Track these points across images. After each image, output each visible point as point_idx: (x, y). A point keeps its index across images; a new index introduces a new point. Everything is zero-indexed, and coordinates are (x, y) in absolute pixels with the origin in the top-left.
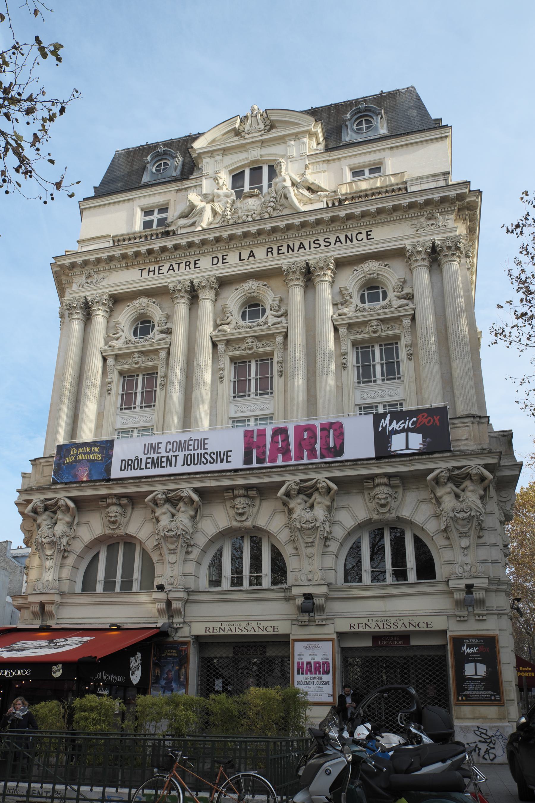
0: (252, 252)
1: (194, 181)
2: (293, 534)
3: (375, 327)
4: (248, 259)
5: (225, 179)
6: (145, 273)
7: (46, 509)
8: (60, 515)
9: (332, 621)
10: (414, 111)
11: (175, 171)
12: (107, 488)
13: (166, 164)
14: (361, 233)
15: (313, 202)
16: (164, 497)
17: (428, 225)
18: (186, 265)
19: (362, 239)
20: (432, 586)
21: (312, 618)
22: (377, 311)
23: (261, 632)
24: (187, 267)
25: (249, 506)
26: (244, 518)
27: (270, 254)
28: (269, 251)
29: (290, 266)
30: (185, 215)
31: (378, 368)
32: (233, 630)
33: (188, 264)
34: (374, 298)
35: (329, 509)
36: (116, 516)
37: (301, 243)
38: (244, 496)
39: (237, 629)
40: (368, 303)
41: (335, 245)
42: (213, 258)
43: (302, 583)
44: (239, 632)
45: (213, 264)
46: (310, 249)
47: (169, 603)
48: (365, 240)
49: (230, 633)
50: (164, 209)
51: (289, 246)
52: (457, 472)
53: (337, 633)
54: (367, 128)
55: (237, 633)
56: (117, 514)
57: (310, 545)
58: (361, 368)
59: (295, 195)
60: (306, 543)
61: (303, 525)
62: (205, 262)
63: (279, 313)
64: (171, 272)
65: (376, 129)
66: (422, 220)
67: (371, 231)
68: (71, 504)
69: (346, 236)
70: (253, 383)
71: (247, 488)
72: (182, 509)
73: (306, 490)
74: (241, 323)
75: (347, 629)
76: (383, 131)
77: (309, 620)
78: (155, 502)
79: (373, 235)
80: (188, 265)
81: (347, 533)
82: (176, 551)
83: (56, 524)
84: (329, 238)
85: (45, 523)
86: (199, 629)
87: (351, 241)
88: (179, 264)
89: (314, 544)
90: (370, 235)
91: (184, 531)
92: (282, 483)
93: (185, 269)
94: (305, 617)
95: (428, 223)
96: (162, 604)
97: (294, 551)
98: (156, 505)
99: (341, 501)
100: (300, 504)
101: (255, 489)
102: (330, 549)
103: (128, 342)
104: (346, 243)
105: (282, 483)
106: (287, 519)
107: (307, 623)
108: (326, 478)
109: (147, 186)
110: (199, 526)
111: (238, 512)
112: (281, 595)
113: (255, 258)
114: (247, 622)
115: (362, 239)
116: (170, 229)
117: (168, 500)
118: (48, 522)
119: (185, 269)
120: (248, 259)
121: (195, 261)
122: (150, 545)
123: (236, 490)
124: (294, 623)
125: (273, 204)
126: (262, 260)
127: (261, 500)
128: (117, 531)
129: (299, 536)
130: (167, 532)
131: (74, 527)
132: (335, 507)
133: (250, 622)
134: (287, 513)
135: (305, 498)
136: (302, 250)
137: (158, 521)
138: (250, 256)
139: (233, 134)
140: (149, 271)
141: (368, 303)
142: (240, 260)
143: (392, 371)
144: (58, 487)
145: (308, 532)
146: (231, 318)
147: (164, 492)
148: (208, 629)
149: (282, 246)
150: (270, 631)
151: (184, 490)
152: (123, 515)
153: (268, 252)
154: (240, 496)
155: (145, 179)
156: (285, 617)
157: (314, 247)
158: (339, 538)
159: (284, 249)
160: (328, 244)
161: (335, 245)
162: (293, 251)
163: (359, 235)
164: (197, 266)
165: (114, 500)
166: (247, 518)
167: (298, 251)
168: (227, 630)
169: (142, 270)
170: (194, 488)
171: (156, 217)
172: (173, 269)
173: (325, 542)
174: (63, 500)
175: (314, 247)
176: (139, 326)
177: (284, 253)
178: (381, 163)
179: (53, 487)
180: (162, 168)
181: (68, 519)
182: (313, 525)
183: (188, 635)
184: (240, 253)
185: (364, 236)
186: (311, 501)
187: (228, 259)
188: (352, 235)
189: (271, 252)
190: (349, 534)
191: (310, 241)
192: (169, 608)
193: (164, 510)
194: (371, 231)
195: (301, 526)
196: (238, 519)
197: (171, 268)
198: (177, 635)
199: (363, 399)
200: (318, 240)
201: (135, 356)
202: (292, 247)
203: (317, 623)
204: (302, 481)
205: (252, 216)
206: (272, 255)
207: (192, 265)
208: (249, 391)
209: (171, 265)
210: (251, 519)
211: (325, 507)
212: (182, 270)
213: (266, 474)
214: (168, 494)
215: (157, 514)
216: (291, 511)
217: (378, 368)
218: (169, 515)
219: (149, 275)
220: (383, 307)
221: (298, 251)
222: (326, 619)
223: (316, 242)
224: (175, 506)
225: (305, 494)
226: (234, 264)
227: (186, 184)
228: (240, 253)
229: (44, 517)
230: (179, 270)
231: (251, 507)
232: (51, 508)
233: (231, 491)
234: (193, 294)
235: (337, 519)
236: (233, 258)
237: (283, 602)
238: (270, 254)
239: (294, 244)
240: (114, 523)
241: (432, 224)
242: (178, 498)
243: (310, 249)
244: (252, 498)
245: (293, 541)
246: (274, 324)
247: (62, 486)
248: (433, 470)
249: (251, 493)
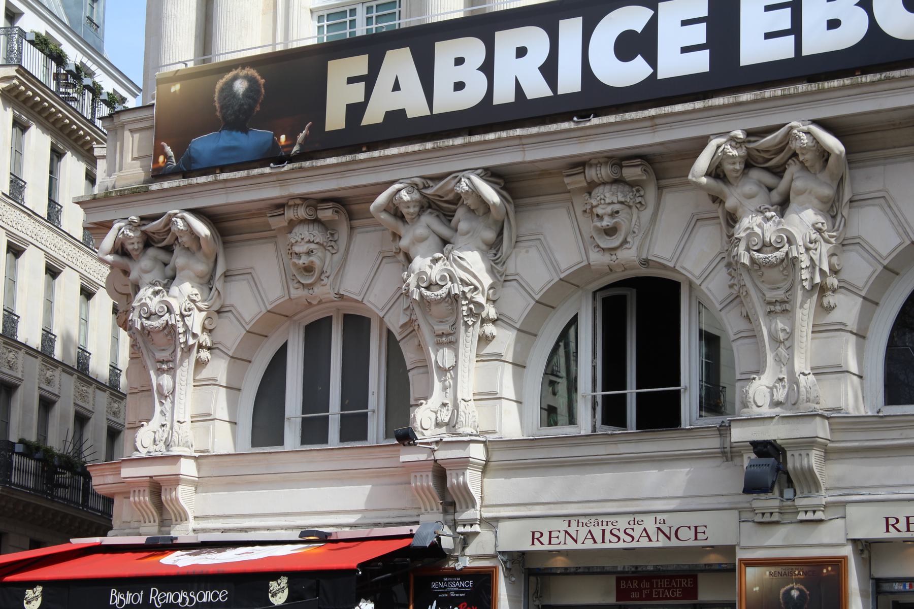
2: (736, 282)
7: (148, 242)
8: (179, 259)
9: (839, 512)
12: (282, 180)
16: (416, 196)
21: (789, 503)
23: (662, 542)
25: (630, 207)
26: (615, 242)
32: (599, 538)
35: (831, 209)
36: (309, 253)
38: (615, 182)
39: (608, 536)
43: (754, 411)
44: (611, 544)
49: (589, 545)
53: (855, 541)
55: (607, 545)
56: (312, 246)
57: (778, 308)
60: (770, 303)
61: (756, 254)
68: (202, 229)
71: (618, 160)
72: (463, 226)
73: (766, 156)
75: (878, 532)
77: (780, 508)
78: (395, 211)
81: (880, 268)
83: (173, 278)
85: (148, 278)
86: (512, 537)
89: (788, 307)
91: (467, 284)
92: (702, 142)
94: (769, 503)
96: (424, 474)
97: (743, 325)
98: (398, 215)
99: (868, 181)
100: (751, 197)
101: (638, 162)
102: (835, 317)
106: (725, 238)
107: (776, 518)
108: (816, 122)
110: (510, 268)
111: (599, 224)
112: (713, 443)
114: (631, 518)
117: (428, 205)
118: (155, 275)
122: (395, 321)
123: (591, 166)
124: (746, 516)
127: (660, 188)
128: (318, 291)
129: (749, 285)
131: (218, 284)
132: (847, 198)
133: (638, 517)
134: (722, 220)
135: (768, 179)
137: (409, 260)
144: (166, 185)
145: (775, 274)
147: (414, 186)
148: (537, 535)
150: (687, 539)
151: (460, 174)
152: (330, 245)
154: (604, 183)
156: (723, 502)
158: (860, 285)
165: (302, 213)
166: (625, 242)
168: (583, 540)
170: (486, 169)
174: (183, 218)
179: (155, 187)
181: (201, 267)
182: (780, 254)
183: (490, 551)
186: (783, 185)
193: (420, 229)
195: (752, 260)
196: (603, 245)
198: (468, 551)
203: (802, 516)
204: (749, 133)
210: (635, 242)
211: (816, 201)
213: (658, 121)
214: (425, 187)
215: (404, 243)
216: (732, 219)
218: (433, 241)
222: (825, 506)
224: (446, 216)
225: (767, 169)
229: (145, 262)
231: (635, 210)
232: (158, 241)
233: (580, 169)
235: (852, 232)
237: (718, 462)
240: (308, 269)
242: (450, 197)
244: (634, 185)
245: (737, 298)
247: (175, 183)
249: (632, 173)
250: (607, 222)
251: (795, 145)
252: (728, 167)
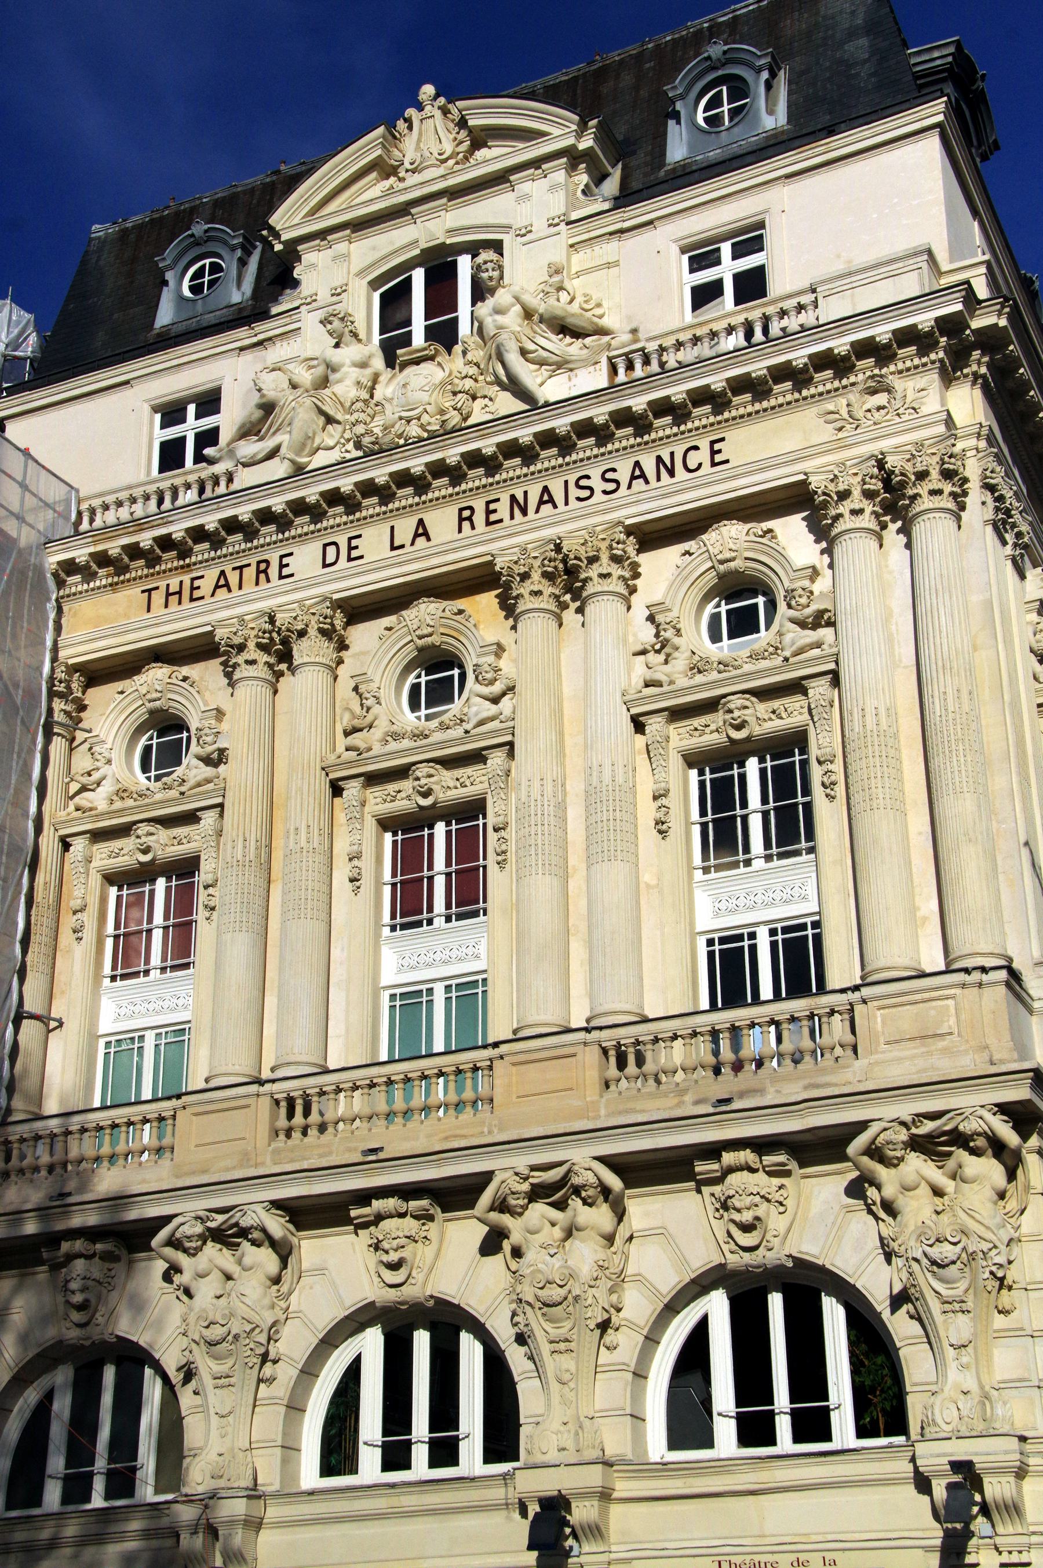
0: (421, 522)
3: (736, 713)
4: (412, 544)
6: (158, 598)
10: (863, 42)
11: (239, 285)
13: (215, 268)
14: (696, 448)
15: (571, 366)
17: (869, 411)
18: (258, 572)
19: (700, 465)
20: (881, 1460)
22: (740, 667)
24: (262, 576)
27: (466, 525)
28: (465, 517)
29: (515, 558)
30: (249, 431)
31: (756, 823)
33: (263, 566)
34: (743, 623)
37: (546, 489)
40: (730, 637)
41: (629, 487)
42: (325, 546)
43: (539, 1458)
45: (325, 565)
46: (567, 504)
48: (706, 468)
50: (209, 402)
51: (513, 498)
52: (928, 1127)
54: (734, 113)
57: (562, 1346)
58: (711, 825)
59: (523, 352)
62: (305, 558)
63: (497, 688)
64: (222, 593)
65: (757, 119)
66: (853, 397)
67: (723, 439)
69: (659, 459)
70: (440, 882)
74: (409, 719)
79: (727, 450)
80: (262, 570)
82: (232, 1380)
84: (614, 470)
87: (671, 473)
88: (241, 568)
90: (719, 451)
93: (257, 584)
95: (866, 407)
103: (122, 793)
104: (659, 479)
105: (486, 1177)
109: (169, 340)
113: (429, 539)
115: (700, 465)
116: (219, 468)
119: (257, 584)
120: (412, 544)
121: (282, 557)
125: (468, 384)
126: (448, 541)
130: (207, 1327)
136: (547, 508)
138: (416, 535)
140: (168, 594)
141: (730, 637)
142: (393, 548)
143: (791, 830)
146: (376, 710)
149: (498, 500)
153: (461, 520)
155: (165, 315)
157: (579, 499)
159: (503, 509)
160: (612, 486)
161: (629, 487)
162: (524, 512)
163: (692, 453)
164: (286, 571)
167: (537, 511)
169: (149, 591)
171: (191, 426)
172: (227, 585)
173: (601, 1337)
175: (579, 499)
176: (155, 742)
177: (501, 521)
178: (761, 225)
180: (206, 279)
184: (392, 528)
185: (702, 456)
187: (363, 546)
188: (672, 454)
189: (469, 519)
190: (672, 1308)
191: (566, 482)
194: (723, 439)
197: (222, 583)
199: (717, 913)
200: (588, 477)
201: (139, 832)
202: (522, 502)
204: (534, 1168)
205: (419, 419)
206: (473, 528)
207: (273, 572)
208: (430, 909)
209: (223, 573)
212: (249, 587)
217: (756, 823)
218: (216, 1276)
219: (166, 606)
220: (754, 656)
221: (537, 511)
223: (583, 482)
226: (380, 554)
227: (264, 329)
228: (392, 528)
230: (240, 588)
234: (281, 651)
236: (373, 541)
238: (466, 525)
239: (526, 493)
241: (879, 408)
243: (567, 504)
246: (481, 723)
250: (394, 1257)
251: (576, 1180)
252: (512, 1202)
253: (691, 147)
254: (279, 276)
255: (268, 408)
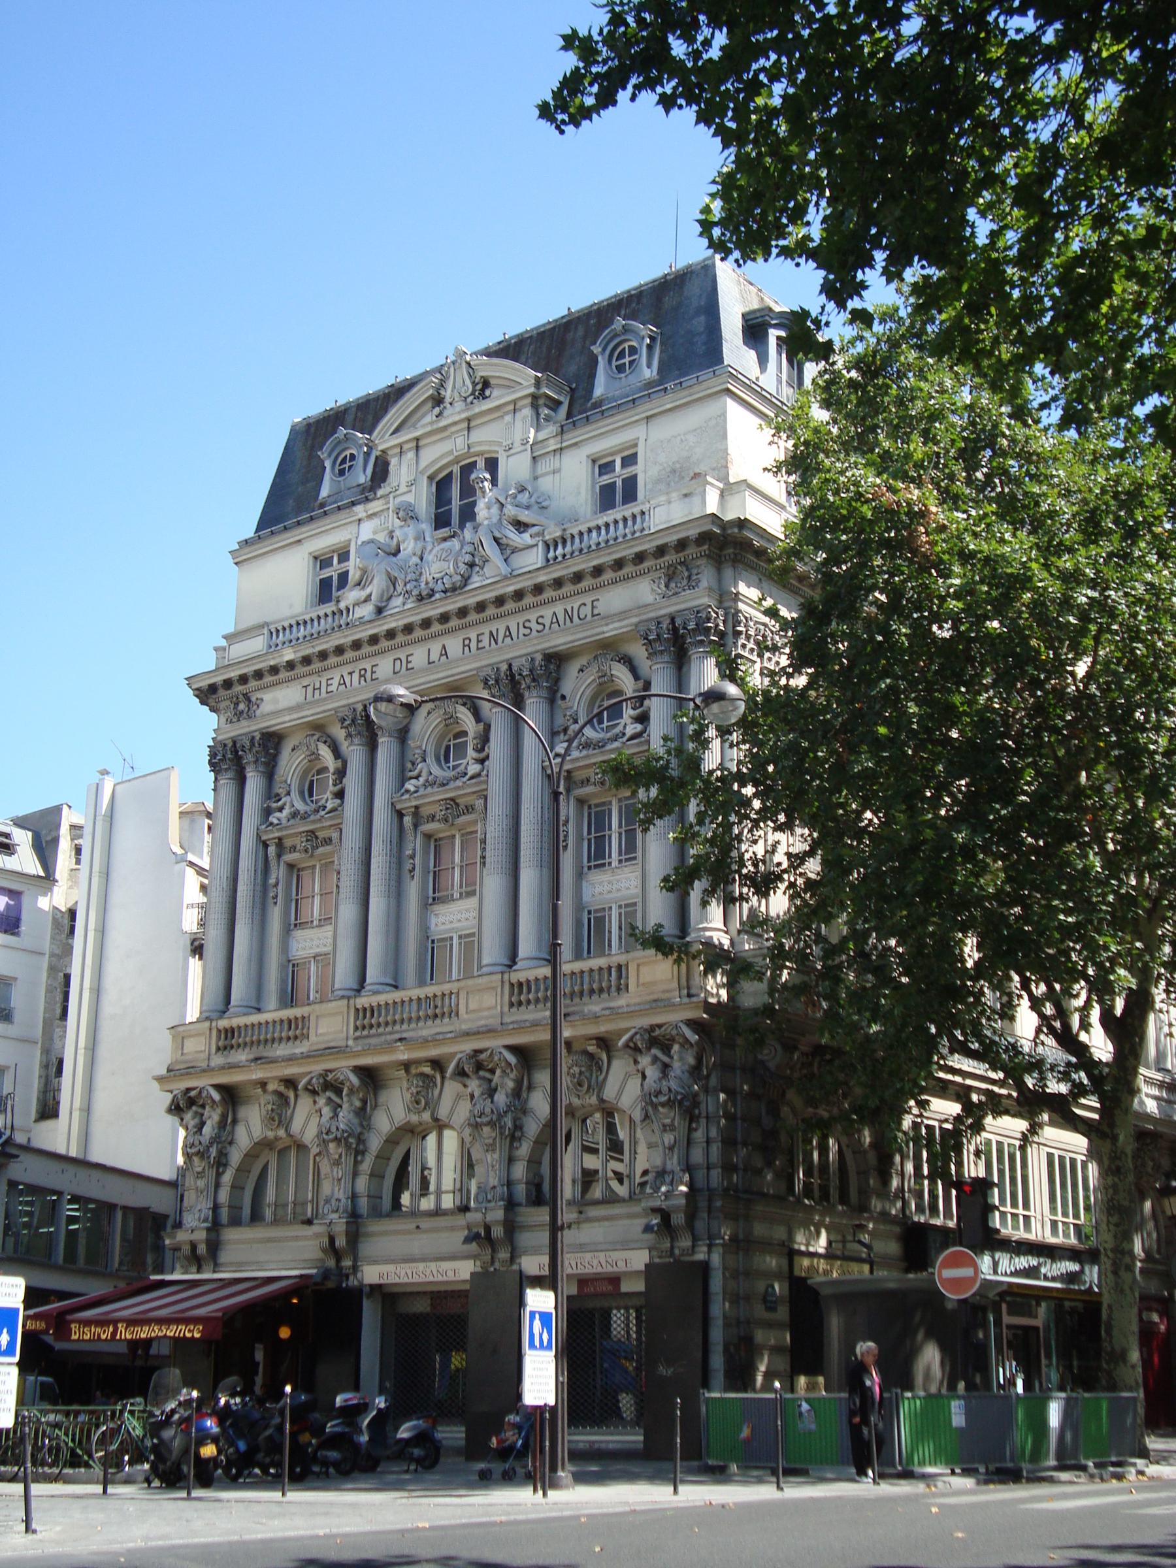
1: (381, 502)
5: (422, 498)
28: (466, 645)
47: (332, 1240)
52: (657, 1032)
59: (496, 540)
76: (648, 373)
139: (430, 405)
159: (485, 641)
192: (331, 1247)
248: (627, 1030)
253: (607, 386)
254: (381, 473)
255: (364, 571)
